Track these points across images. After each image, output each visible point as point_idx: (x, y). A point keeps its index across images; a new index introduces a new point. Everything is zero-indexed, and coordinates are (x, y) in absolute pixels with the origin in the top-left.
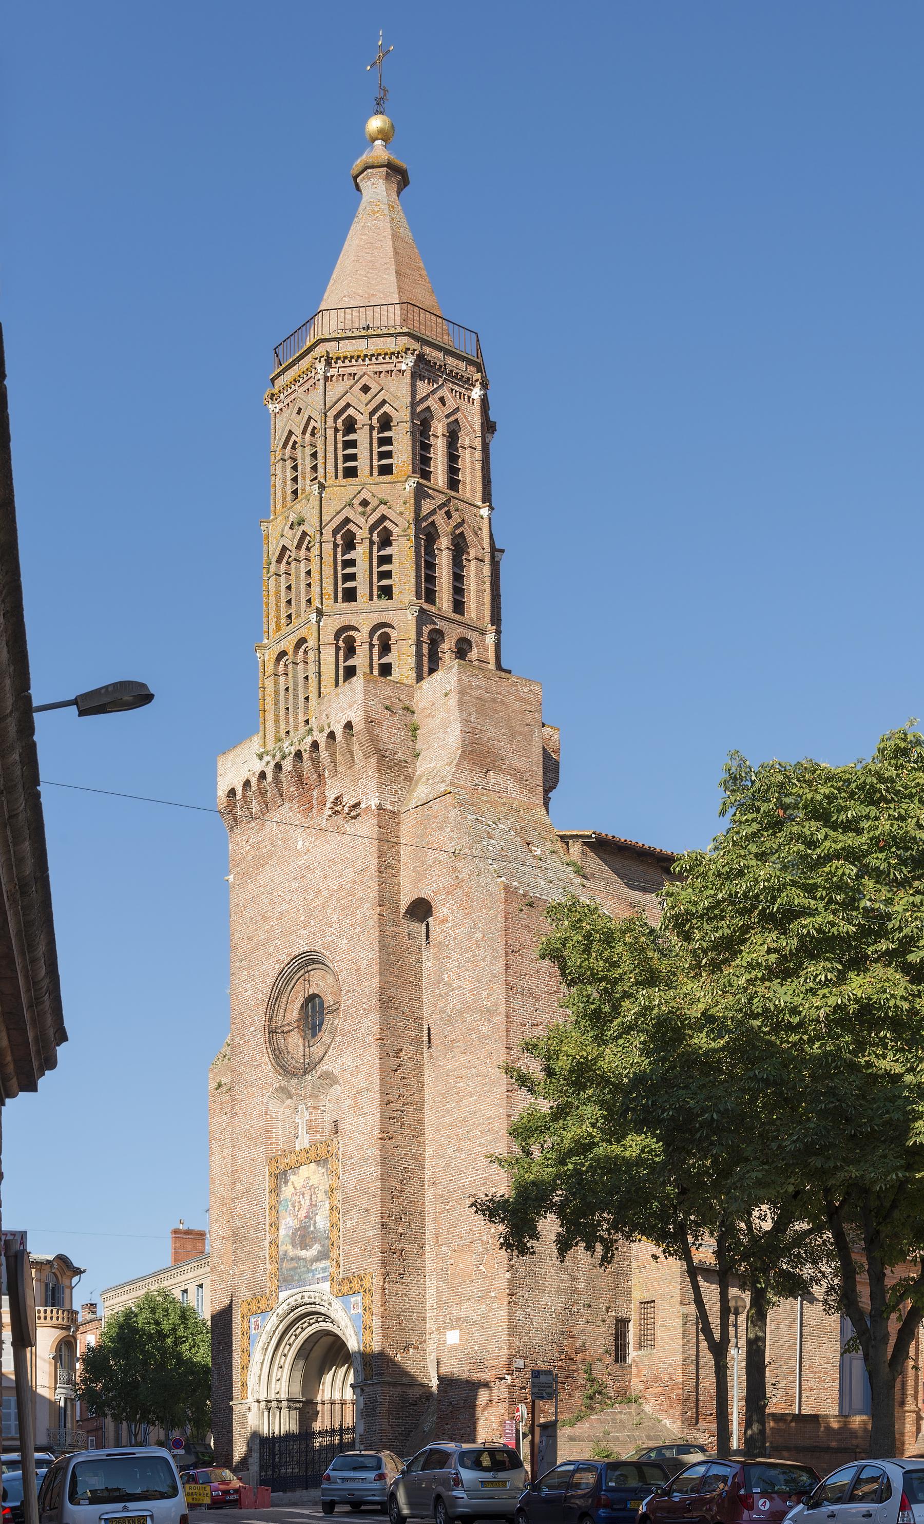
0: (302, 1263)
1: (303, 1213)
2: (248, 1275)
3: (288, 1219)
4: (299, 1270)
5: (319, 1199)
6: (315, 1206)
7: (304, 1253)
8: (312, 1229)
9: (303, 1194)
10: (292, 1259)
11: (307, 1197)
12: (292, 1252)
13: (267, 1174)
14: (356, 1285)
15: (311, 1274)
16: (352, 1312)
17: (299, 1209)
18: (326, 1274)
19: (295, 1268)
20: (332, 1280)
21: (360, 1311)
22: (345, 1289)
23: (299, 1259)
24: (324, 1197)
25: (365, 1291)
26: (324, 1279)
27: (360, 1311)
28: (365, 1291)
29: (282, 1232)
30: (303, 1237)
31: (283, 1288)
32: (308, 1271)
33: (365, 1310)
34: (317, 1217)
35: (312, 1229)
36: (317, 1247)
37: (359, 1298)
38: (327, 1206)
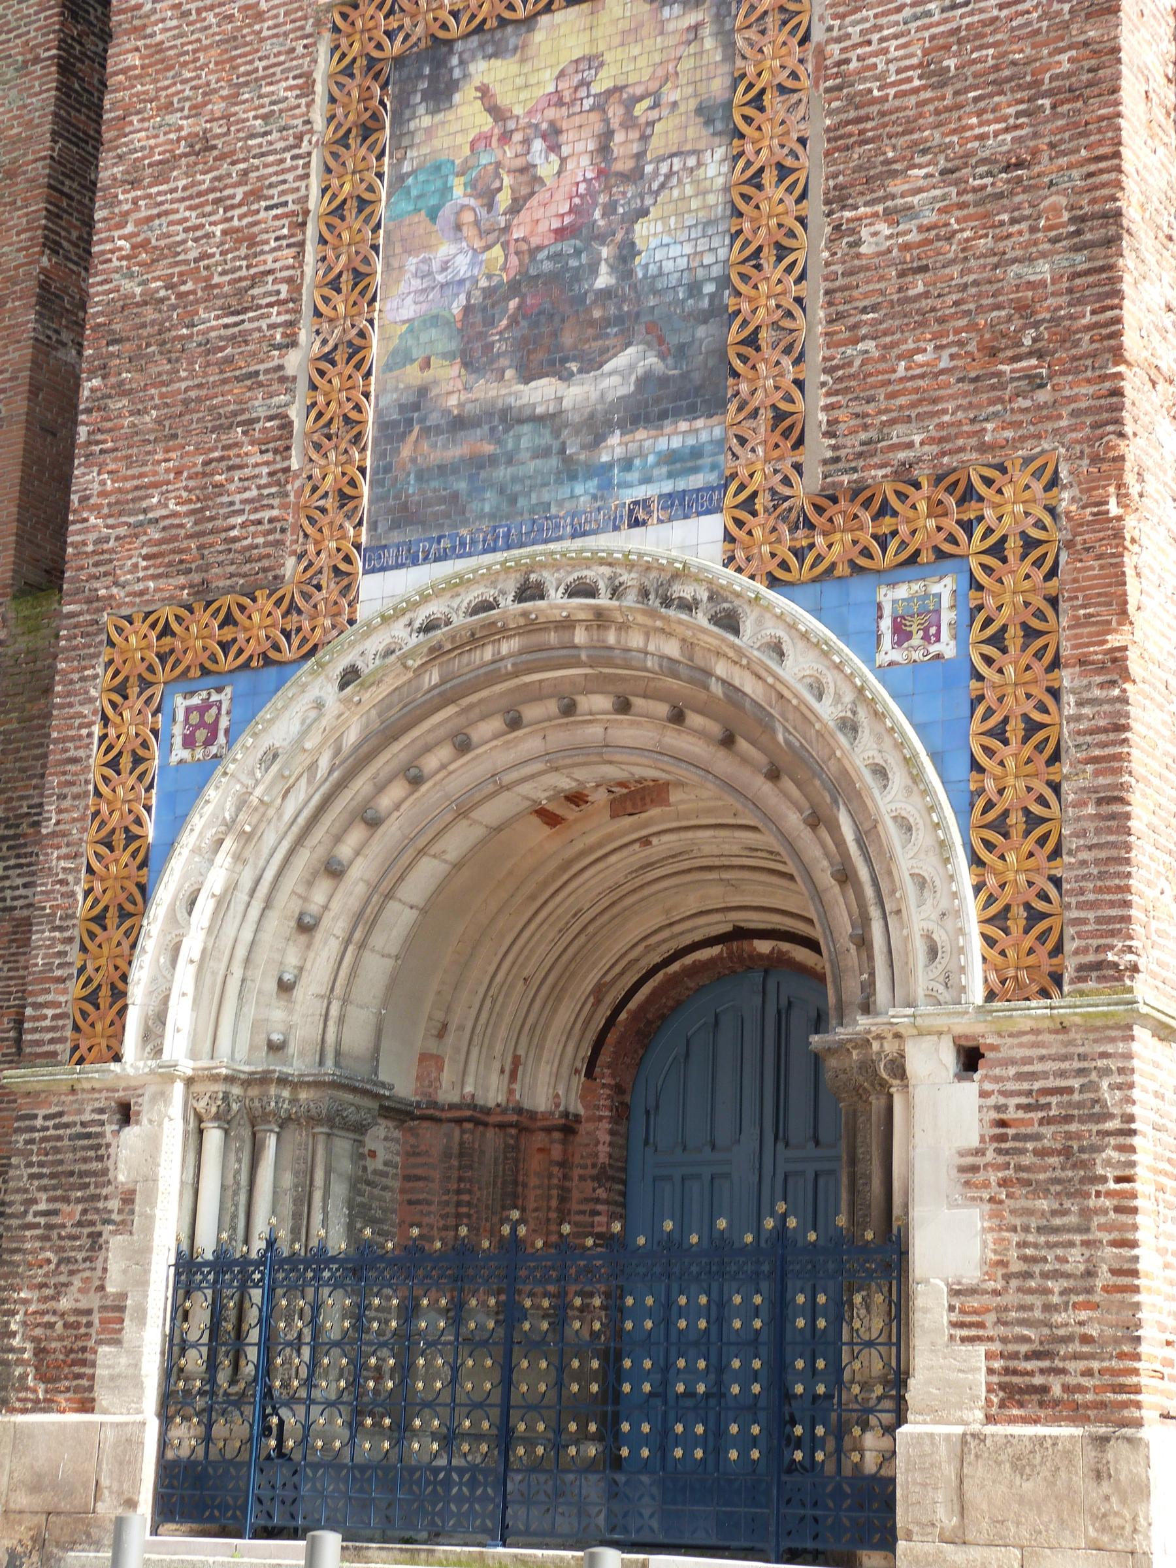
0: (527, 438)
1: (542, 220)
2: (170, 503)
3: (446, 250)
4: (502, 473)
5: (657, 145)
6: (635, 175)
7: (541, 393)
8: (604, 279)
9: (552, 136)
10: (459, 424)
11: (579, 146)
12: (453, 390)
13: (323, 67)
14: (921, 522)
15: (583, 490)
16: (889, 653)
17: (515, 208)
18: (697, 481)
19: (478, 463)
20: (749, 505)
21: (947, 647)
22: (836, 548)
23: (508, 418)
24: (696, 132)
25: (998, 550)
26: (682, 505)
27: (947, 647)
28: (998, 550)
29: (399, 306)
30: (542, 316)
31: (390, 556)
32: (570, 471)
33: (998, 640)
34: (641, 229)
35: (604, 279)
36: (627, 366)
37: (944, 588)
38: (715, 167)
